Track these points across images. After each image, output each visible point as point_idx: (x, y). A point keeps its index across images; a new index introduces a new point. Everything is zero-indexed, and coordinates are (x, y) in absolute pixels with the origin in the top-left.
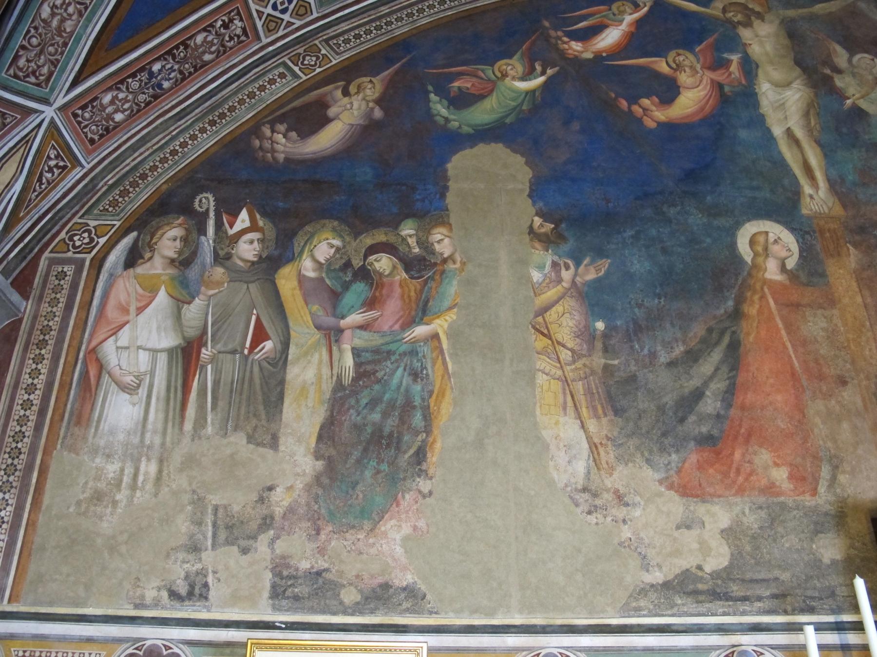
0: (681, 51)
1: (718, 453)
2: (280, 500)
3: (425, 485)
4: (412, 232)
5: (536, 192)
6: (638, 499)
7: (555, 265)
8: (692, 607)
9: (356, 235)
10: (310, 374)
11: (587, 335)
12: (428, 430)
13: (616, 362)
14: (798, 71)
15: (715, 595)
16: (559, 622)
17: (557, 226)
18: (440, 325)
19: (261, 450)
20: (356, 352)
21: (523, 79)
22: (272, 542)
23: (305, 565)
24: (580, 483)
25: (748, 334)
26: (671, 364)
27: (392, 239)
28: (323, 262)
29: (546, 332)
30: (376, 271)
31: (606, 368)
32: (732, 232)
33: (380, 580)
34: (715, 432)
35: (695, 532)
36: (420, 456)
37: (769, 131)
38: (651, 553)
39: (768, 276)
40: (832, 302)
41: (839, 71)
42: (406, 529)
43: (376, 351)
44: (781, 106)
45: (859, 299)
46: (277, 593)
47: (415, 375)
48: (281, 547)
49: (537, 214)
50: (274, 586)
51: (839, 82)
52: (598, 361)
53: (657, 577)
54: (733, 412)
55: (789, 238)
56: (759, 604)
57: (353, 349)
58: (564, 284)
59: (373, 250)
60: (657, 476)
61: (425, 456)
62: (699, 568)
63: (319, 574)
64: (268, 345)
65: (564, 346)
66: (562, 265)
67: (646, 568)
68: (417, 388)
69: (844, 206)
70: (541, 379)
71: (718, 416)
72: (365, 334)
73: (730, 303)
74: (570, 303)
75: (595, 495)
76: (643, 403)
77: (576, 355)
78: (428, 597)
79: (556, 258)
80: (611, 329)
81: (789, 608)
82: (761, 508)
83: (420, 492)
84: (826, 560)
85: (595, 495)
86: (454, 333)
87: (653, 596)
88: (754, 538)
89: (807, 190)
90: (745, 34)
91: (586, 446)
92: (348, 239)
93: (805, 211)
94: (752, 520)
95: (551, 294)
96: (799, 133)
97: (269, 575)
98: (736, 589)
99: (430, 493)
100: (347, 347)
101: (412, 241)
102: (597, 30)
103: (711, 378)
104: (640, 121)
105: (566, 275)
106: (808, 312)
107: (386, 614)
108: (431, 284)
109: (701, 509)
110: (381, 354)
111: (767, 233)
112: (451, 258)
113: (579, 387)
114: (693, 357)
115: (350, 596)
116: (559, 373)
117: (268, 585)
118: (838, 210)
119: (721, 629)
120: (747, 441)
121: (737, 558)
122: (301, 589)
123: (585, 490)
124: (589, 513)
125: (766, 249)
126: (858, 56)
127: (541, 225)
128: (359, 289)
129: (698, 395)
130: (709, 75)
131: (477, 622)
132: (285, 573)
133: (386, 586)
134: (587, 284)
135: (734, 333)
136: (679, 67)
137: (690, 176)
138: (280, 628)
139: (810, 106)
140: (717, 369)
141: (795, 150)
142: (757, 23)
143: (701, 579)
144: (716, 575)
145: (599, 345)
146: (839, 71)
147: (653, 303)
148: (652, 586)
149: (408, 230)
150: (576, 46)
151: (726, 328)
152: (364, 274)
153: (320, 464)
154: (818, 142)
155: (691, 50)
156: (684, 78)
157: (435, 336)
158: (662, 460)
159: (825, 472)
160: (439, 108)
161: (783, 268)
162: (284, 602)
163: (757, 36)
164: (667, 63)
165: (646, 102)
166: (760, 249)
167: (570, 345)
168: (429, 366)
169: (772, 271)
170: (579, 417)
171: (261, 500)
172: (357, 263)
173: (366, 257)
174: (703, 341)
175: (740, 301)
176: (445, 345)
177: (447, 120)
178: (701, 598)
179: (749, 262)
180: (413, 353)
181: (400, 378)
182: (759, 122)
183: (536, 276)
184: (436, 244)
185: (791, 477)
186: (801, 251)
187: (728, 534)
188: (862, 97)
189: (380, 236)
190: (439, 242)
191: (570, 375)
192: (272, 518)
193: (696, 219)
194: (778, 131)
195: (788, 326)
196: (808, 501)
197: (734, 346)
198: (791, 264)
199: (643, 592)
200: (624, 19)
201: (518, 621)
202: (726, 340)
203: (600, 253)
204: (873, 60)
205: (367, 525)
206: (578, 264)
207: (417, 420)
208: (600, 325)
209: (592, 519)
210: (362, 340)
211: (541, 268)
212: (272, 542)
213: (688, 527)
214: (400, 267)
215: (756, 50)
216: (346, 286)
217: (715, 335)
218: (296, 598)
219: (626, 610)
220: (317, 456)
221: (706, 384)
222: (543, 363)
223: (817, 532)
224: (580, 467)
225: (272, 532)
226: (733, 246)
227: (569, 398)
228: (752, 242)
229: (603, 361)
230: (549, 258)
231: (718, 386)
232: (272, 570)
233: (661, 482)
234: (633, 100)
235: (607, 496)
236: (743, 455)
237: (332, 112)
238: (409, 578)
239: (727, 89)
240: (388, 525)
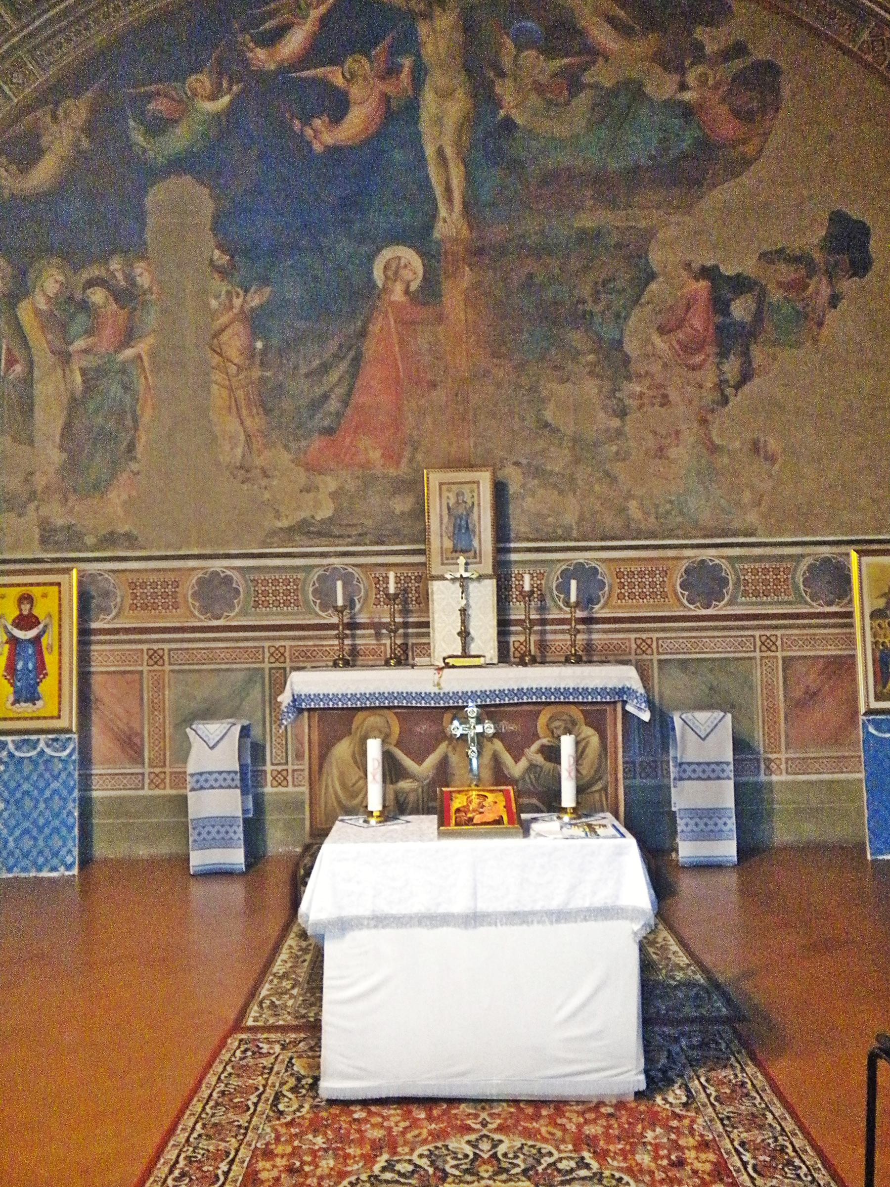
0: (357, 56)
1: (333, 441)
2: (40, 481)
3: (134, 466)
4: (119, 267)
5: (218, 225)
6: (277, 473)
7: (229, 293)
8: (306, 542)
9: (76, 270)
10: (51, 389)
11: (251, 353)
12: (136, 429)
13: (268, 374)
14: (463, 77)
15: (320, 534)
16: (221, 552)
17: (232, 257)
18: (142, 347)
19: (22, 447)
20: (83, 372)
21: (213, 97)
22: (37, 508)
23: (60, 522)
24: (238, 464)
25: (368, 350)
26: (307, 376)
27: (104, 273)
28: (51, 296)
29: (219, 351)
30: (93, 303)
31: (261, 378)
32: (371, 258)
33: (109, 529)
34: (334, 426)
35: (312, 495)
36: (131, 447)
37: (422, 150)
38: (282, 509)
39: (393, 298)
40: (440, 319)
41: (502, 74)
42: (124, 496)
43: (97, 370)
44: (438, 121)
45: (462, 316)
46: (44, 541)
47: (126, 388)
48: (44, 511)
49: (218, 247)
50: (41, 536)
51: (498, 90)
52: (256, 373)
53: (285, 523)
54: (349, 411)
55: (417, 263)
56: (349, 540)
57: (81, 369)
58: (235, 311)
59: (91, 283)
60: (290, 457)
61: (134, 445)
62: (313, 517)
63: (69, 528)
64: (18, 368)
65: (231, 362)
66: (234, 294)
67: (278, 517)
68: (128, 398)
69: (471, 228)
70: (214, 387)
71: (339, 415)
72: (90, 358)
73: (359, 323)
74: (238, 327)
75: (247, 471)
76: (286, 404)
77: (240, 368)
78: (140, 539)
79: (229, 288)
80: (266, 346)
81: (368, 542)
82: (358, 477)
83: (132, 471)
84: (397, 512)
85: (247, 471)
86: (153, 354)
87: (281, 535)
88: (351, 497)
89: (443, 212)
90: (423, 29)
91: (242, 437)
92: (70, 273)
93: (436, 235)
94: (351, 486)
95: (224, 319)
96: (449, 152)
97: (37, 530)
98: (336, 531)
99: (138, 473)
100: (75, 367)
101: (119, 276)
102: (282, 31)
103: (336, 385)
104: (309, 144)
105: (237, 302)
106: (419, 328)
107: (113, 550)
108: (138, 313)
109: (319, 479)
110: (101, 372)
111: (399, 258)
112: (150, 288)
113: (240, 394)
114: (325, 368)
115: (90, 540)
116: (227, 383)
117: (37, 536)
118: (465, 232)
119: (323, 555)
120: (355, 432)
121: (338, 510)
122: (60, 537)
123: (241, 467)
124: (243, 482)
125: (396, 273)
126: (526, 53)
127: (220, 258)
128: (81, 318)
129: (325, 397)
130: (382, 87)
131: (168, 554)
132: (47, 528)
133: (112, 533)
134: (253, 309)
135: (358, 347)
136: (351, 78)
137: (347, 204)
138: (47, 562)
139: (466, 118)
140: (340, 379)
141: (441, 170)
142: (438, 11)
143: (312, 525)
144: (322, 522)
145: (257, 361)
146: (502, 74)
147: (301, 325)
148: (281, 529)
149: (115, 264)
150: (261, 54)
151: (352, 346)
152: (84, 306)
153: (65, 456)
154: (463, 161)
155: (367, 55)
156: (355, 92)
157: (139, 357)
158: (293, 445)
159: (407, 454)
160: (138, 138)
161: (407, 292)
162: (50, 547)
163: (434, 31)
164: (343, 74)
165: (317, 122)
166: (390, 273)
167: (236, 361)
168: (135, 380)
169: (397, 294)
170: (239, 415)
171: (26, 481)
172: (78, 296)
173: (84, 289)
174: (335, 356)
175: (367, 321)
176: (146, 364)
177: (145, 151)
178: (312, 536)
179: (381, 286)
180: (123, 371)
181: (115, 389)
182: (415, 142)
183: (214, 303)
184: (138, 278)
185: (383, 455)
186: (425, 272)
187: (334, 495)
188: (516, 106)
189: (95, 271)
190: (141, 275)
191: (235, 384)
192: (35, 493)
193: (345, 246)
194: (430, 151)
195: (402, 342)
196: (392, 472)
197: (357, 360)
198: (414, 287)
199: (274, 533)
200: (308, 16)
201: (196, 551)
202: (352, 354)
203: (265, 281)
204: (537, 58)
205: (97, 495)
206: (246, 291)
207: (129, 422)
208: (259, 345)
209: (245, 487)
210: (89, 361)
211: (217, 297)
212: (37, 508)
213: (308, 491)
214: (111, 299)
215: (430, 51)
216: (72, 317)
217: (344, 350)
218: (56, 543)
219: (264, 544)
220: (62, 448)
221: (331, 390)
222: (217, 376)
223: (394, 493)
224: (239, 451)
225: (36, 503)
226: (370, 273)
227: (233, 403)
228: (386, 268)
229: (260, 373)
230: (224, 288)
231: (340, 391)
232: (39, 526)
233: (292, 461)
234: (307, 121)
235: (257, 472)
236: (351, 442)
237: (45, 141)
238: (127, 528)
239: (394, 104)
240: (112, 495)
